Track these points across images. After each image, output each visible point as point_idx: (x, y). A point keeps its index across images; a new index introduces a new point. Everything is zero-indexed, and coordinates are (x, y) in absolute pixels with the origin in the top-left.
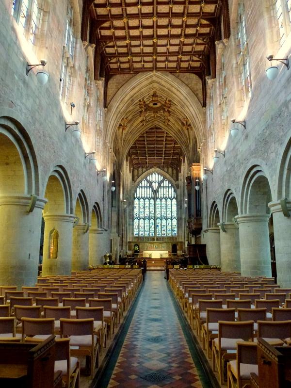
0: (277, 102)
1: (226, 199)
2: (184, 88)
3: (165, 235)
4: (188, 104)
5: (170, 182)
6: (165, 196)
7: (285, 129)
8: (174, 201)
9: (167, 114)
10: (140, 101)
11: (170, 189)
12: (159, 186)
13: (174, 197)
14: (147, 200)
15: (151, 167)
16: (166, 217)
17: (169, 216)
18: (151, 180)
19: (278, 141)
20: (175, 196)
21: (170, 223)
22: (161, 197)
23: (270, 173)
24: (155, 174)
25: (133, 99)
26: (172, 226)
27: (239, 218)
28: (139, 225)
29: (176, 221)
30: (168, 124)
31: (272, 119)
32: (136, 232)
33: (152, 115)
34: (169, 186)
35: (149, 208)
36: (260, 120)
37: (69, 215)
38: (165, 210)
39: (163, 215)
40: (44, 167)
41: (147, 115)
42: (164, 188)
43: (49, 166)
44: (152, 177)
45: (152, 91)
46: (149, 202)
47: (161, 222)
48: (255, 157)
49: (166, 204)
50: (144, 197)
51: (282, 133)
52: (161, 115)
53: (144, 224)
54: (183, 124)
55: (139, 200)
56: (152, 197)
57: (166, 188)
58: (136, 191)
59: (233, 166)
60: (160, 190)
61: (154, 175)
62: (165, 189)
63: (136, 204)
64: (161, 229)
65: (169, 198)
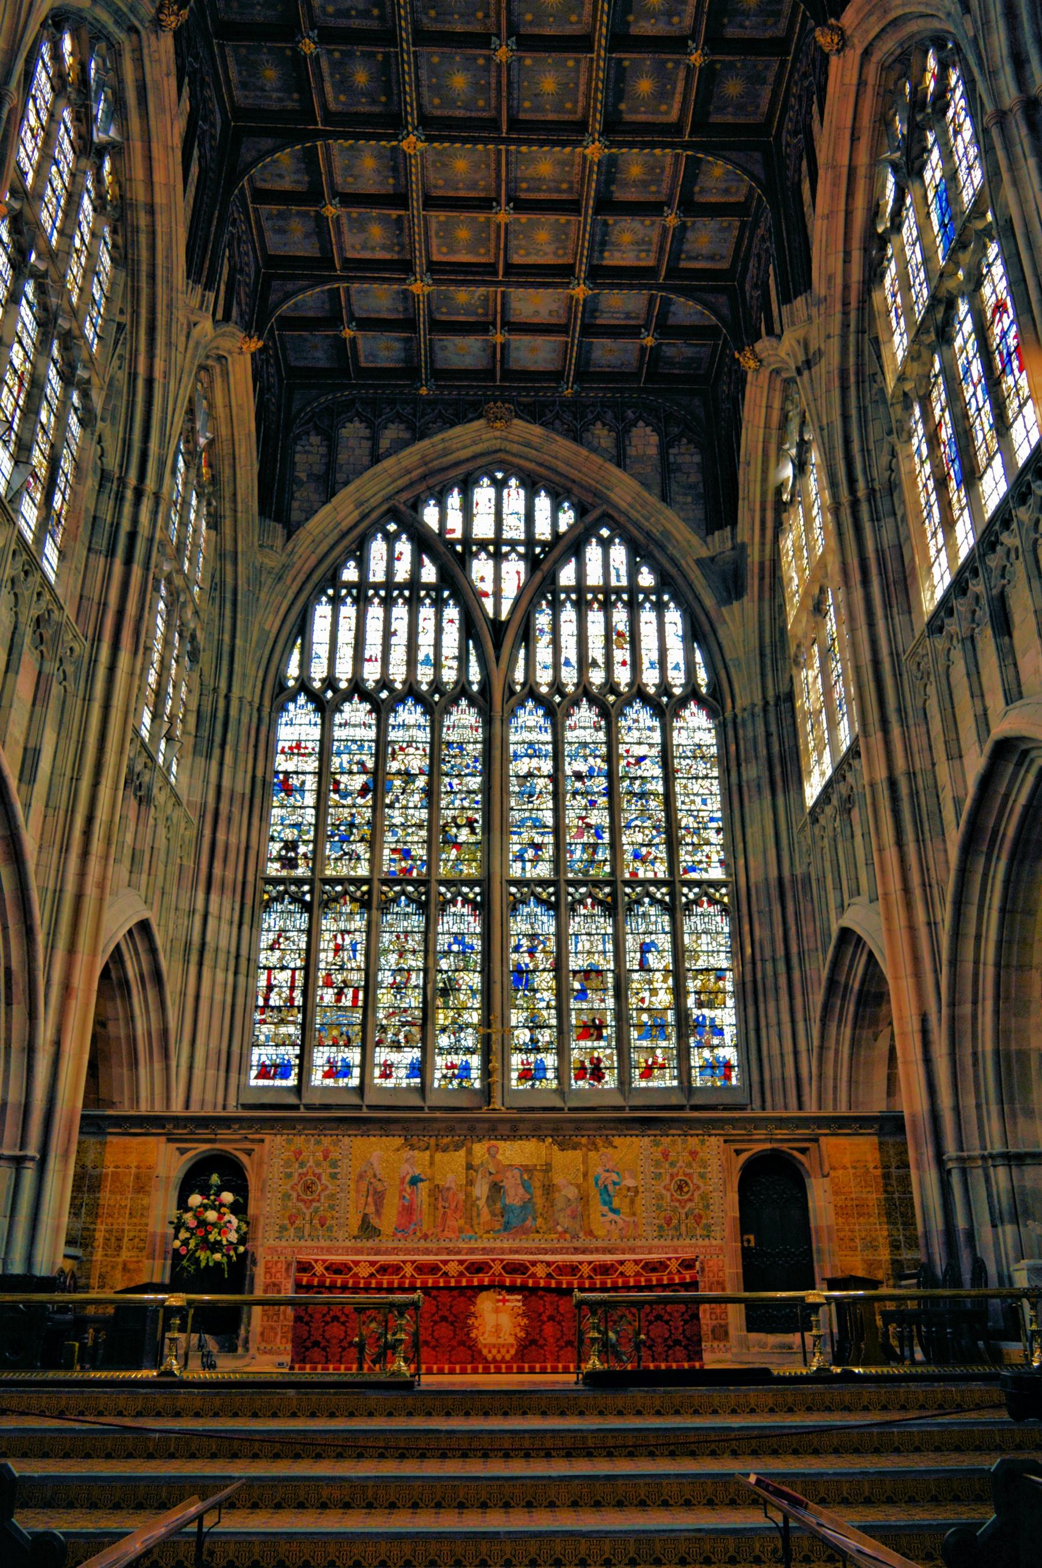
3: (610, 1081)
6: (597, 677)
11: (647, 617)
13: (692, 693)
14: (410, 714)
20: (702, 676)
21: (664, 942)
22: (557, 686)
24: (500, 486)
28: (309, 967)
34: (633, 588)
35: (431, 794)
38: (599, 817)
42: (581, 607)
47: (561, 936)
49: (610, 758)
50: (384, 683)
53: (372, 955)
56: (462, 689)
57: (607, 607)
58: (303, 627)
60: (543, 620)
61: (484, 494)
62: (595, 619)
64: (562, 1011)
65: (638, 692)
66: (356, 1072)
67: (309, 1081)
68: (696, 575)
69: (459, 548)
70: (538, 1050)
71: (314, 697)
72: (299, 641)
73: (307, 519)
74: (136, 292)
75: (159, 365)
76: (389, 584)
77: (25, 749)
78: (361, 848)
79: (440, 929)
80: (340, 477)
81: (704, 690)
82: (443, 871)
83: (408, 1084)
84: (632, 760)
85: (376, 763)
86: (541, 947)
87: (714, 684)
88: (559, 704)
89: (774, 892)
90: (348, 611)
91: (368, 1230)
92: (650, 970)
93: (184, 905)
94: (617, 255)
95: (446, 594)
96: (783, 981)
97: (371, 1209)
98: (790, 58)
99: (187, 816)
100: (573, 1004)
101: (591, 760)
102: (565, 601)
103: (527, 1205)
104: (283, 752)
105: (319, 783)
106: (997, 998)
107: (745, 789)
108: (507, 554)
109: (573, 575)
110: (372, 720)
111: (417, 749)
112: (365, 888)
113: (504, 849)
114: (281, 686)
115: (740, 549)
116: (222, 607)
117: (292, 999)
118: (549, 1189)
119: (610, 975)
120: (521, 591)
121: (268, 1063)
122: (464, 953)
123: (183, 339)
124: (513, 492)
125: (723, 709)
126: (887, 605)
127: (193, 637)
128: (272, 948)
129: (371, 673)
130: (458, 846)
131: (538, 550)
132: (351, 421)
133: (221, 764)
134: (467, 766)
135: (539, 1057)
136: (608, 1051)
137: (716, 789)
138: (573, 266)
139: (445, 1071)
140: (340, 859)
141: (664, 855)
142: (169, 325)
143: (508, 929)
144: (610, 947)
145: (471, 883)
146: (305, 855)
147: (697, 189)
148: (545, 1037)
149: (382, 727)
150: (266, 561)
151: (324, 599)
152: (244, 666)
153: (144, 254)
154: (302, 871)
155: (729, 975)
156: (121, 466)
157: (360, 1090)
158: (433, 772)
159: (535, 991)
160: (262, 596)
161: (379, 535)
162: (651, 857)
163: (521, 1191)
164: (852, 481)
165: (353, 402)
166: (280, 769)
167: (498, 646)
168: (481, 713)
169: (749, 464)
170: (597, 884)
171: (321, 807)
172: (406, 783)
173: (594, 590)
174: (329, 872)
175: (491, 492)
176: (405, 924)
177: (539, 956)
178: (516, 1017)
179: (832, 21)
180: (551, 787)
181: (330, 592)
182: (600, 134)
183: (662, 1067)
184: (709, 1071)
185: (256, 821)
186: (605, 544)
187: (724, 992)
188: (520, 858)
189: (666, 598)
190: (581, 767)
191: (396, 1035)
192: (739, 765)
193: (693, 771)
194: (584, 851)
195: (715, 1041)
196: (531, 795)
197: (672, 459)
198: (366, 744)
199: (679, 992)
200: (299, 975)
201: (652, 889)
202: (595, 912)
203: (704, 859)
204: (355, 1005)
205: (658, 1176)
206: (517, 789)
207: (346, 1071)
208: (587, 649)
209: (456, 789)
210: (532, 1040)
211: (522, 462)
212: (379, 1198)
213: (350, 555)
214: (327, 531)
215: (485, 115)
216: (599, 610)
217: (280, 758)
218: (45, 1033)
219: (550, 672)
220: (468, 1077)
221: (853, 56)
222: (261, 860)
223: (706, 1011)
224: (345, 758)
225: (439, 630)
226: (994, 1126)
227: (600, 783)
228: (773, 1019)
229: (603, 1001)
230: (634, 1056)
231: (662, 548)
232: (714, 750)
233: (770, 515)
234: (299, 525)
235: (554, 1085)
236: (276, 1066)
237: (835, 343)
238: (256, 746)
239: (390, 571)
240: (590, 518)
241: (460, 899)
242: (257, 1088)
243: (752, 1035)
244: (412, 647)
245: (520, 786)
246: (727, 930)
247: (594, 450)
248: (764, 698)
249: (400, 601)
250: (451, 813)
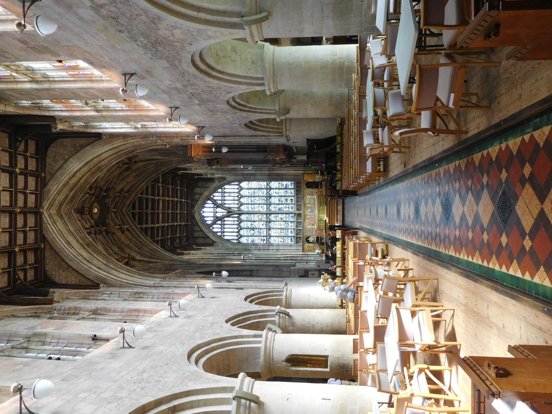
0: (94, 22)
1: (241, 107)
2: (71, 166)
3: (293, 198)
4: (96, 161)
5: (215, 191)
6: (236, 198)
7: (136, 12)
8: (244, 184)
9: (111, 194)
10: (89, 234)
11: (226, 191)
15: (194, 218)
16: (266, 197)
17: (265, 192)
18: (212, 219)
19: (154, 23)
20: (236, 183)
21: (275, 190)
22: (238, 204)
23: (204, 39)
24: (204, 212)
25: (87, 245)
26: (279, 189)
27: (269, 89)
29: (272, 182)
30: (127, 192)
31: (120, 31)
32: (288, 241)
33: (113, 215)
34: (222, 192)
35: (254, 221)
36: (124, 51)
37: (263, 339)
38: (257, 198)
39: (263, 202)
40: (190, 380)
41: (112, 224)
42: (224, 200)
43: (189, 372)
45: (74, 214)
46: (244, 221)
48: (180, 61)
50: (237, 228)
51: (144, 18)
52: (112, 202)
54: (127, 169)
55: (241, 237)
57: (224, 196)
58: (229, 240)
59: (193, 96)
60: (227, 206)
61: (205, 214)
62: (226, 198)
63: (248, 240)
64: (284, 204)
65: (239, 192)
68: (221, 184)
71: (240, 238)
76: (221, 228)
78: (262, 230)
80: (205, 236)
82: (265, 219)
87: (237, 182)
90: (225, 234)
100: (283, 202)
103: (311, 209)
110: (243, 230)
114: (238, 242)
120: (222, 208)
148: (287, 206)
154: (265, 238)
157: (294, 229)
158: (251, 221)
165: (191, 234)
167: (232, 212)
171: (256, 236)
173: (222, 198)
174: (265, 235)
178: (285, 210)
186: (214, 196)
190: (250, 200)
199: (282, 189)
207: (291, 231)
212: (310, 224)
225: (229, 221)
227: (252, 198)
239: (219, 228)
247: (200, 198)
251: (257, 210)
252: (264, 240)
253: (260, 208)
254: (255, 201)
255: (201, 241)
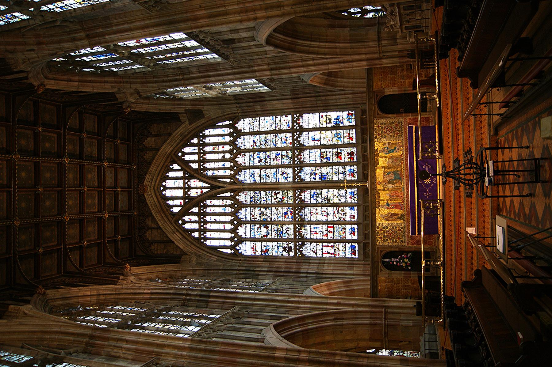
3: (354, 150)
6: (228, 156)
8: (244, 125)
11: (207, 140)
12: (199, 174)
14: (242, 214)
15: (144, 201)
16: (293, 149)
17: (290, 140)
20: (227, 123)
21: (311, 134)
22: (231, 168)
24: (165, 188)
26: (321, 129)
29: (306, 116)
35: (267, 206)
38: (273, 154)
39: (286, 161)
44: (173, 198)
46: (246, 206)
47: (310, 165)
49: (254, 151)
50: (231, 222)
55: (241, 240)
57: (205, 153)
58: (215, 248)
60: (209, 173)
61: (168, 193)
62: (209, 157)
63: (254, 248)
66: (353, 226)
67: (356, 240)
68: (194, 125)
69: (187, 200)
70: (345, 171)
71: (237, 244)
72: (219, 250)
73: (180, 248)
74: (124, 299)
75: (146, 291)
77: (271, 319)
78: (285, 227)
79: (309, 202)
81: (231, 122)
83: (357, 210)
84: (255, 144)
85: (257, 224)
86: (314, 171)
88: (237, 168)
89: (296, 101)
90: (208, 235)
91: (402, 217)
92: (320, 138)
93: (305, 279)
94: (94, 152)
95: (202, 204)
96: (323, 98)
97: (396, 217)
98: (40, 100)
99: (278, 280)
100: (331, 161)
101: (254, 157)
102: (203, 166)
103: (394, 173)
104: (255, 253)
105: (264, 241)
106: (335, 42)
107: (263, 109)
108: (188, 185)
109: (195, 164)
110: (244, 226)
111: (253, 211)
112: (297, 226)
113: (284, 183)
115: (187, 111)
116: (210, 274)
117: (332, 246)
118: (389, 167)
119: (322, 150)
120: (200, 180)
121: (351, 252)
122: (316, 195)
123: (137, 285)
124: (167, 184)
125: (237, 116)
126: (217, 70)
127: (222, 281)
128: (316, 253)
129: (228, 227)
130: (283, 198)
131: (186, 175)
132: (146, 236)
133: (260, 271)
134: (258, 196)
135: (347, 171)
136: (345, 150)
137: (263, 118)
138: (98, 166)
139: (352, 199)
140: (288, 233)
141: (285, 134)
142: (133, 289)
143: (309, 181)
144: (313, 150)
145: (294, 194)
146: (287, 244)
147: (75, 127)
148: (341, 169)
149: (246, 222)
150: (194, 261)
151: (205, 242)
152: (229, 266)
153: (112, 297)
154: (292, 245)
155: (321, 114)
156: (179, 301)
158: (260, 206)
159: (327, 173)
160: (206, 261)
161: (183, 226)
162: (285, 138)
163: (390, 175)
164: (176, 80)
166: (260, 253)
167: (220, 187)
168: (241, 192)
169: (160, 109)
170: (294, 154)
171: (272, 240)
172: (264, 214)
173: (199, 157)
174: (292, 237)
175: (167, 191)
176: (308, 213)
177: (317, 172)
178: (335, 178)
179: (36, 88)
180: (264, 170)
181: (202, 240)
182: (62, 158)
183: (349, 134)
184: (350, 120)
185: (277, 260)
186: (184, 154)
187: (326, 116)
188: (286, 178)
189: (201, 134)
190: (257, 160)
191: (342, 214)
192: (256, 111)
193: (258, 125)
194: (284, 159)
195: (341, 118)
196: (267, 176)
197: (156, 133)
198: (252, 227)
199: (326, 129)
200: (324, 244)
201: (295, 138)
202: (303, 155)
203: (285, 122)
204: (333, 227)
205: (385, 137)
206: (265, 180)
207: (353, 229)
208: (219, 159)
209: (265, 199)
210: (342, 174)
211: (158, 181)
213: (190, 235)
214: (183, 242)
215: (57, 195)
216: (206, 156)
217: (257, 254)
218: (350, 309)
219: (227, 171)
220: (354, 192)
221: (46, 82)
222: (289, 257)
223: (332, 121)
224: (256, 233)
226: (370, 44)
227: (262, 154)
228: (335, 101)
229: (330, 152)
230: (346, 143)
231: (186, 136)
232: (251, 119)
233: (176, 103)
234: (182, 250)
235: (355, 167)
236: (352, 250)
237: (132, 86)
238: (253, 261)
239: (195, 222)
240: (176, 159)
241: (300, 197)
242: (358, 255)
243: (339, 107)
244: (220, 214)
245: (264, 179)
246: (307, 115)
247: (153, 158)
248: (235, 104)
249: (205, 218)
250: (273, 200)
251: (273, 180)
252: (290, 248)
253: (279, 176)
254: (268, 160)
255: (158, 249)
